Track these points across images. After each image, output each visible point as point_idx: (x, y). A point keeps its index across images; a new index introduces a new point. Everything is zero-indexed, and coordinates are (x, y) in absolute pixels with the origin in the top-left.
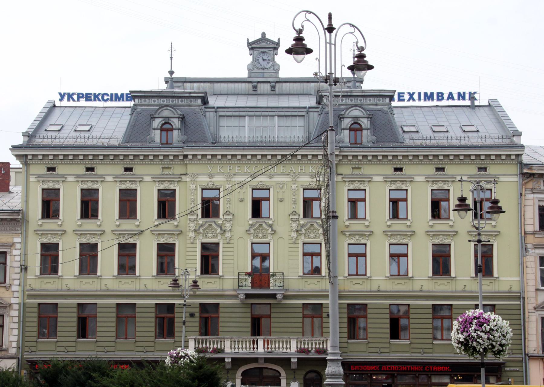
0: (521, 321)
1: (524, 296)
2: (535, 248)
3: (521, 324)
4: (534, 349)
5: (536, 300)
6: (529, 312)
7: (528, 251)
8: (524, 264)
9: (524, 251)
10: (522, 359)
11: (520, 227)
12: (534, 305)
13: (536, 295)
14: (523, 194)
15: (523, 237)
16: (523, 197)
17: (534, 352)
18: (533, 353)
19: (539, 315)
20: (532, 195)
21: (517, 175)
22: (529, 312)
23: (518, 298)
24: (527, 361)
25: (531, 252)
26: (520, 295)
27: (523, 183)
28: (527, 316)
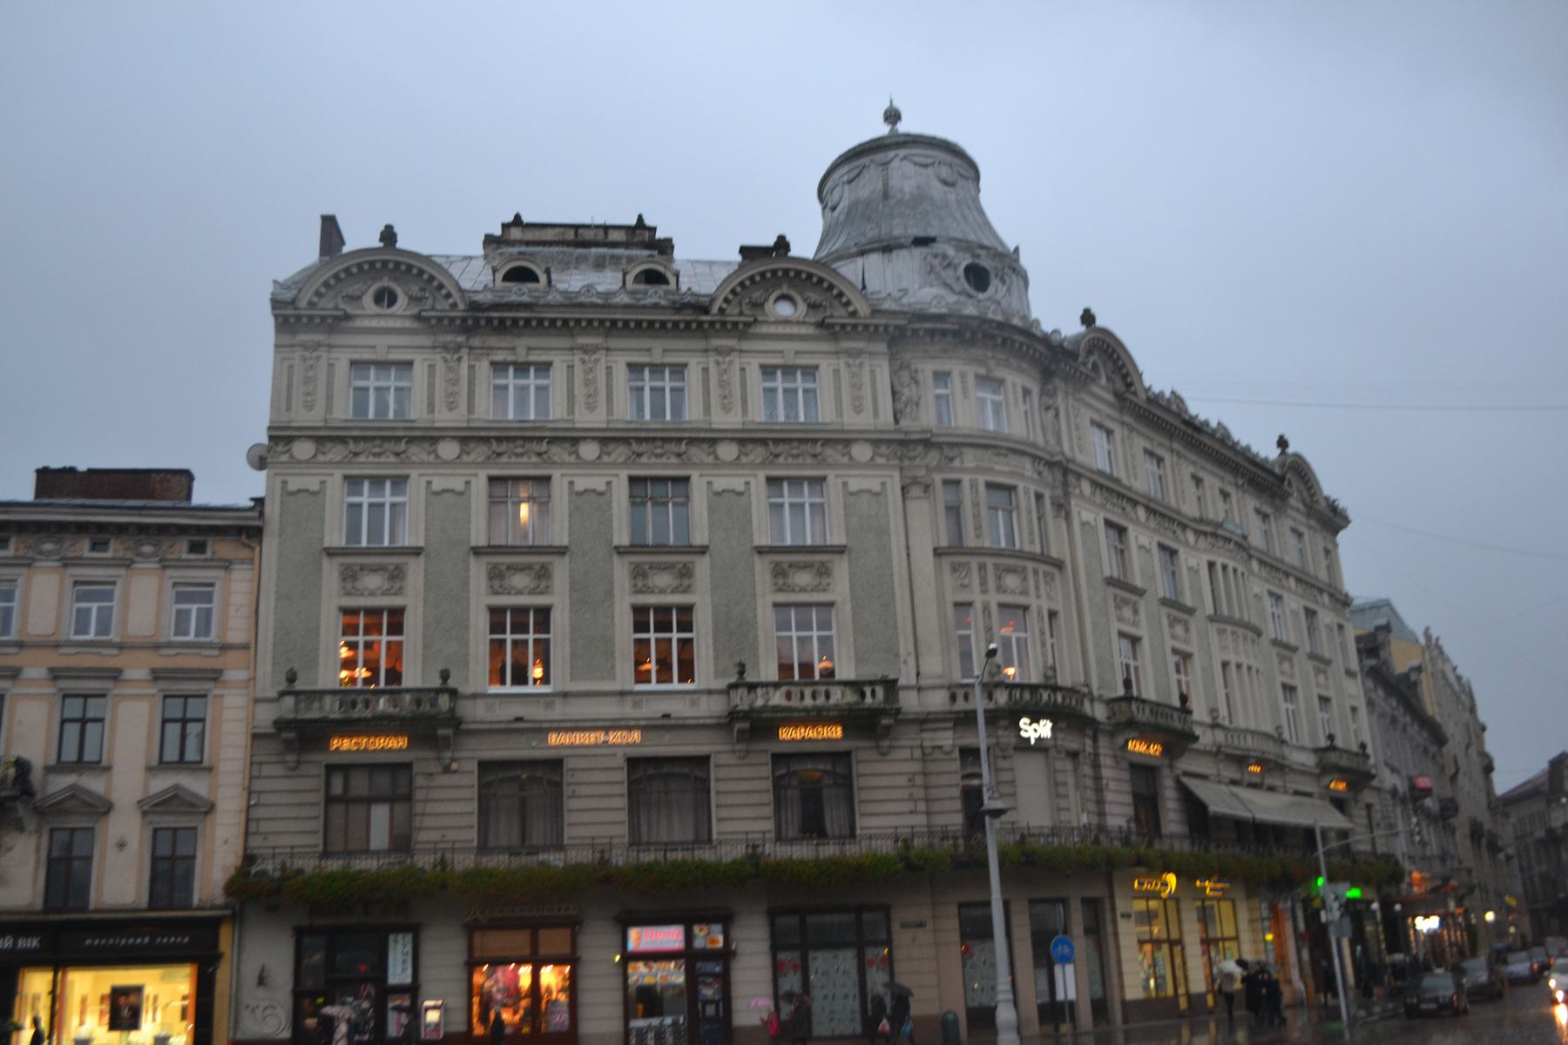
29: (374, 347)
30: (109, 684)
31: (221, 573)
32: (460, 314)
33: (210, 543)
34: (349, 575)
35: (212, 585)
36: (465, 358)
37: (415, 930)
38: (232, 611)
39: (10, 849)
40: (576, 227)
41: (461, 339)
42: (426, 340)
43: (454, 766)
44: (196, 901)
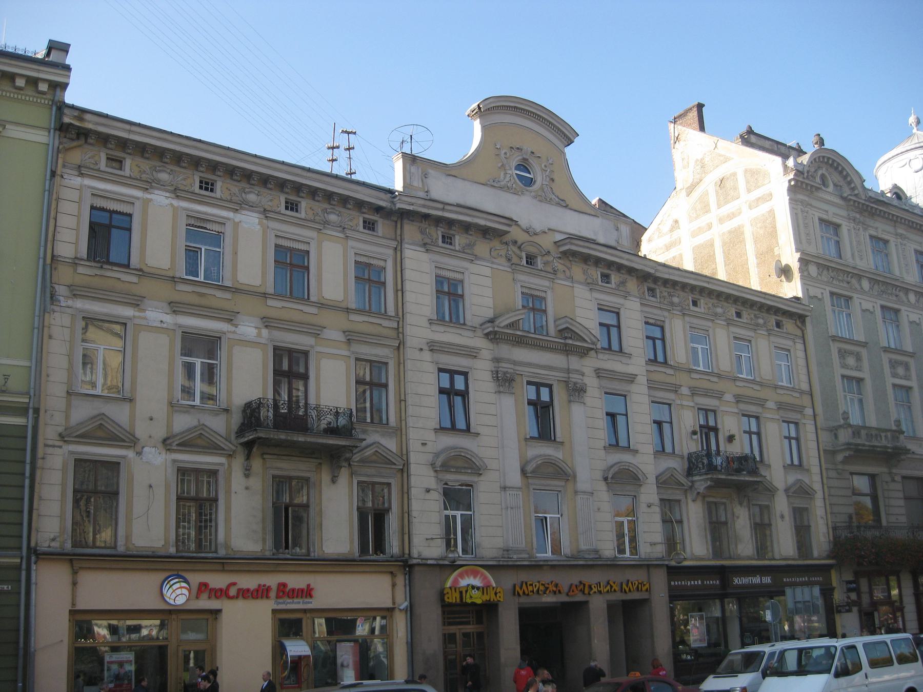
0: (25, 467)
1: (36, 406)
2: (74, 295)
3: (24, 474)
4: (52, 536)
5: (67, 417)
6: (46, 445)
7: (59, 301)
8: (46, 329)
9: (48, 299)
10: (19, 561)
11: (43, 243)
12: (60, 429)
13: (69, 405)
14: (59, 172)
15: (49, 266)
16: (58, 178)
17: (53, 544)
18: (49, 547)
19: (71, 453)
20: (79, 179)
21: (49, 132)
22: (46, 445)
23: (22, 411)
24: (34, 567)
25: (63, 304)
26: (27, 400)
27: (61, 147)
28: (40, 453)
29: (827, 211)
30: (759, 410)
31: (790, 343)
32: (863, 202)
33: (784, 323)
34: (842, 354)
35: (789, 350)
36: (861, 229)
37: (897, 574)
38: (800, 367)
39: (738, 517)
40: (778, 143)
41: (858, 216)
42: (844, 213)
43: (896, 478)
44: (816, 554)
